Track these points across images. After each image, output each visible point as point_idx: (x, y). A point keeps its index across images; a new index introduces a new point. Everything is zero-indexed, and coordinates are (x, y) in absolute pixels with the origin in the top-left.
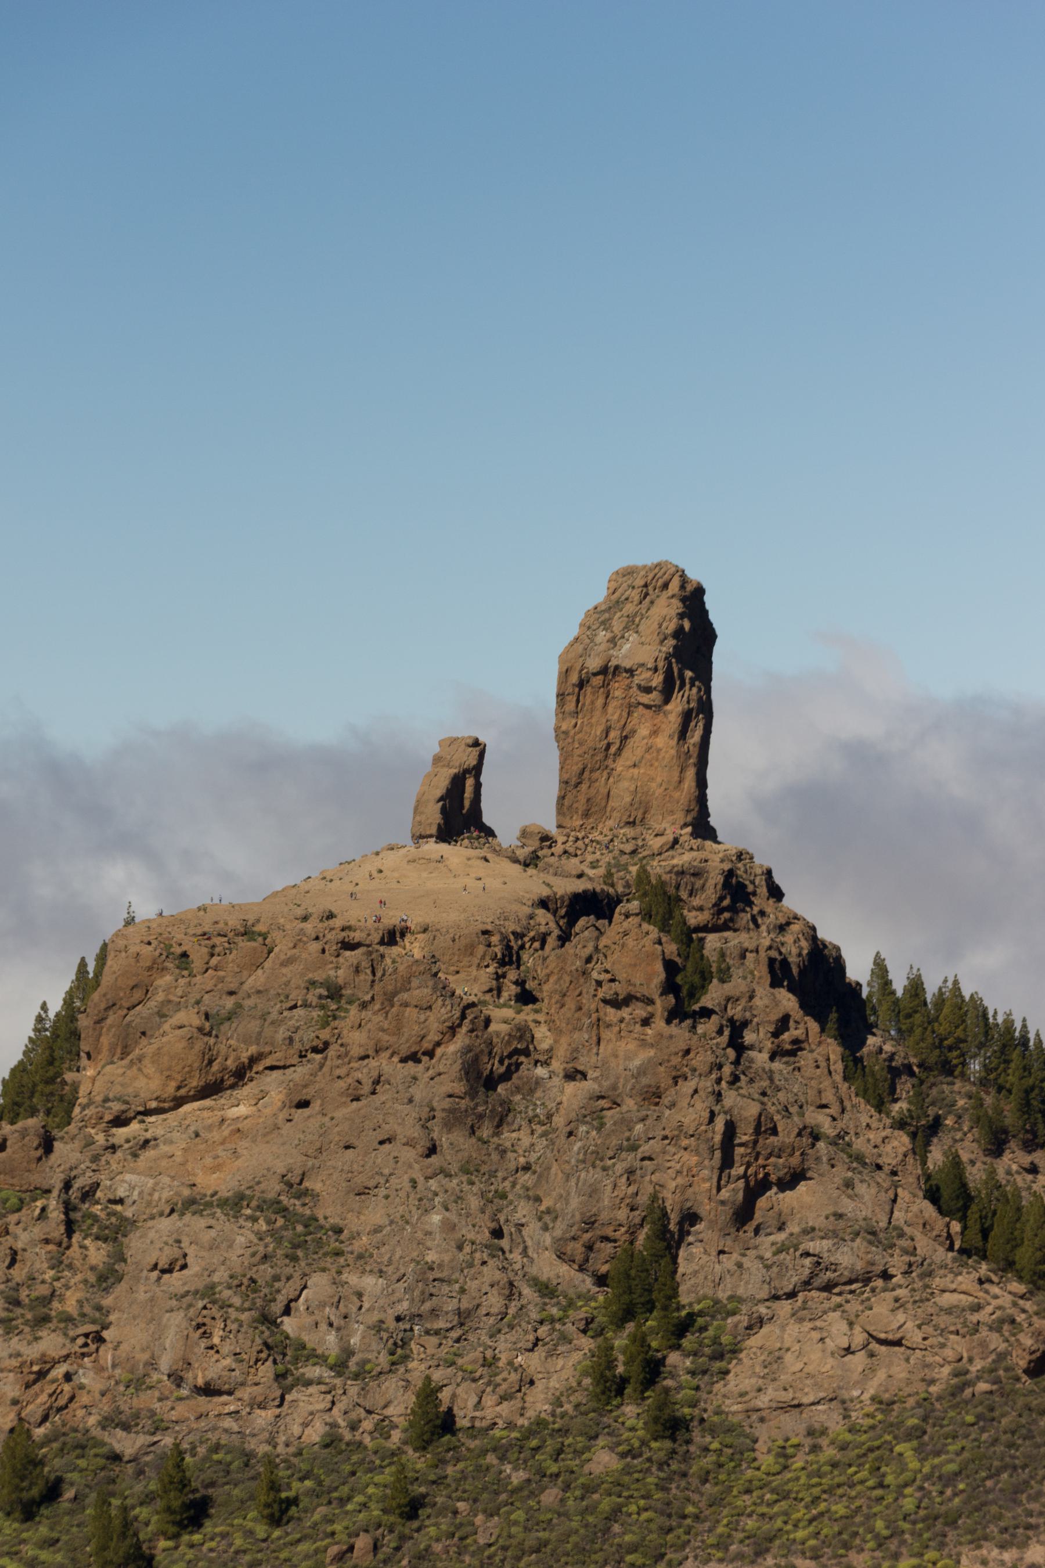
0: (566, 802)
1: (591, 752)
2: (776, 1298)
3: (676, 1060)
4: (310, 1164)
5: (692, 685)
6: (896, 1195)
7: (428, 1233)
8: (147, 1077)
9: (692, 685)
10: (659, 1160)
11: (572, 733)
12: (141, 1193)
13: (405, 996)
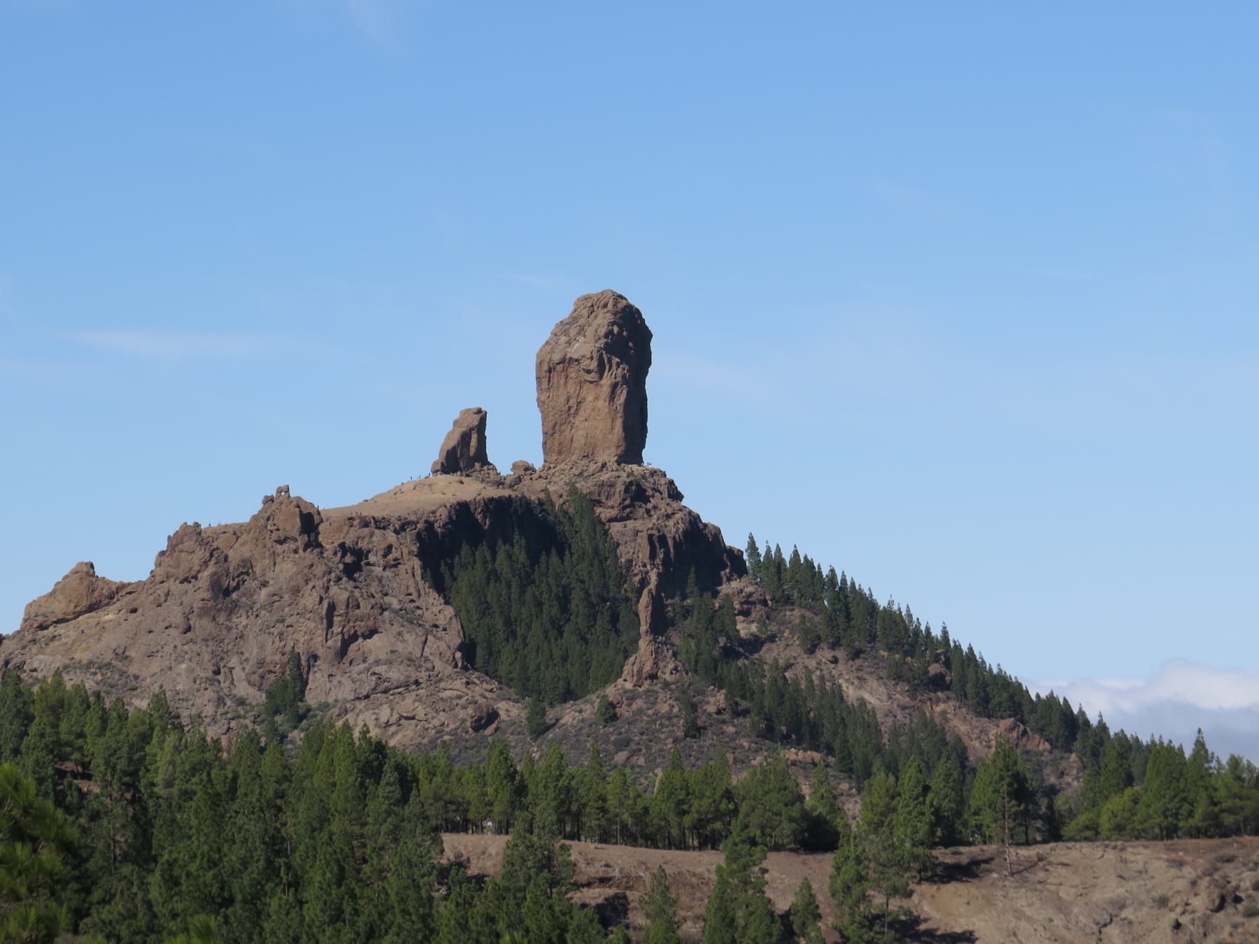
2: (359, 699)
3: (306, 571)
4: (129, 642)
5: (618, 366)
6: (426, 639)
7: (179, 674)
8: (59, 602)
9: (618, 366)
10: (295, 627)
11: (547, 402)
12: (45, 664)
13: (181, 546)
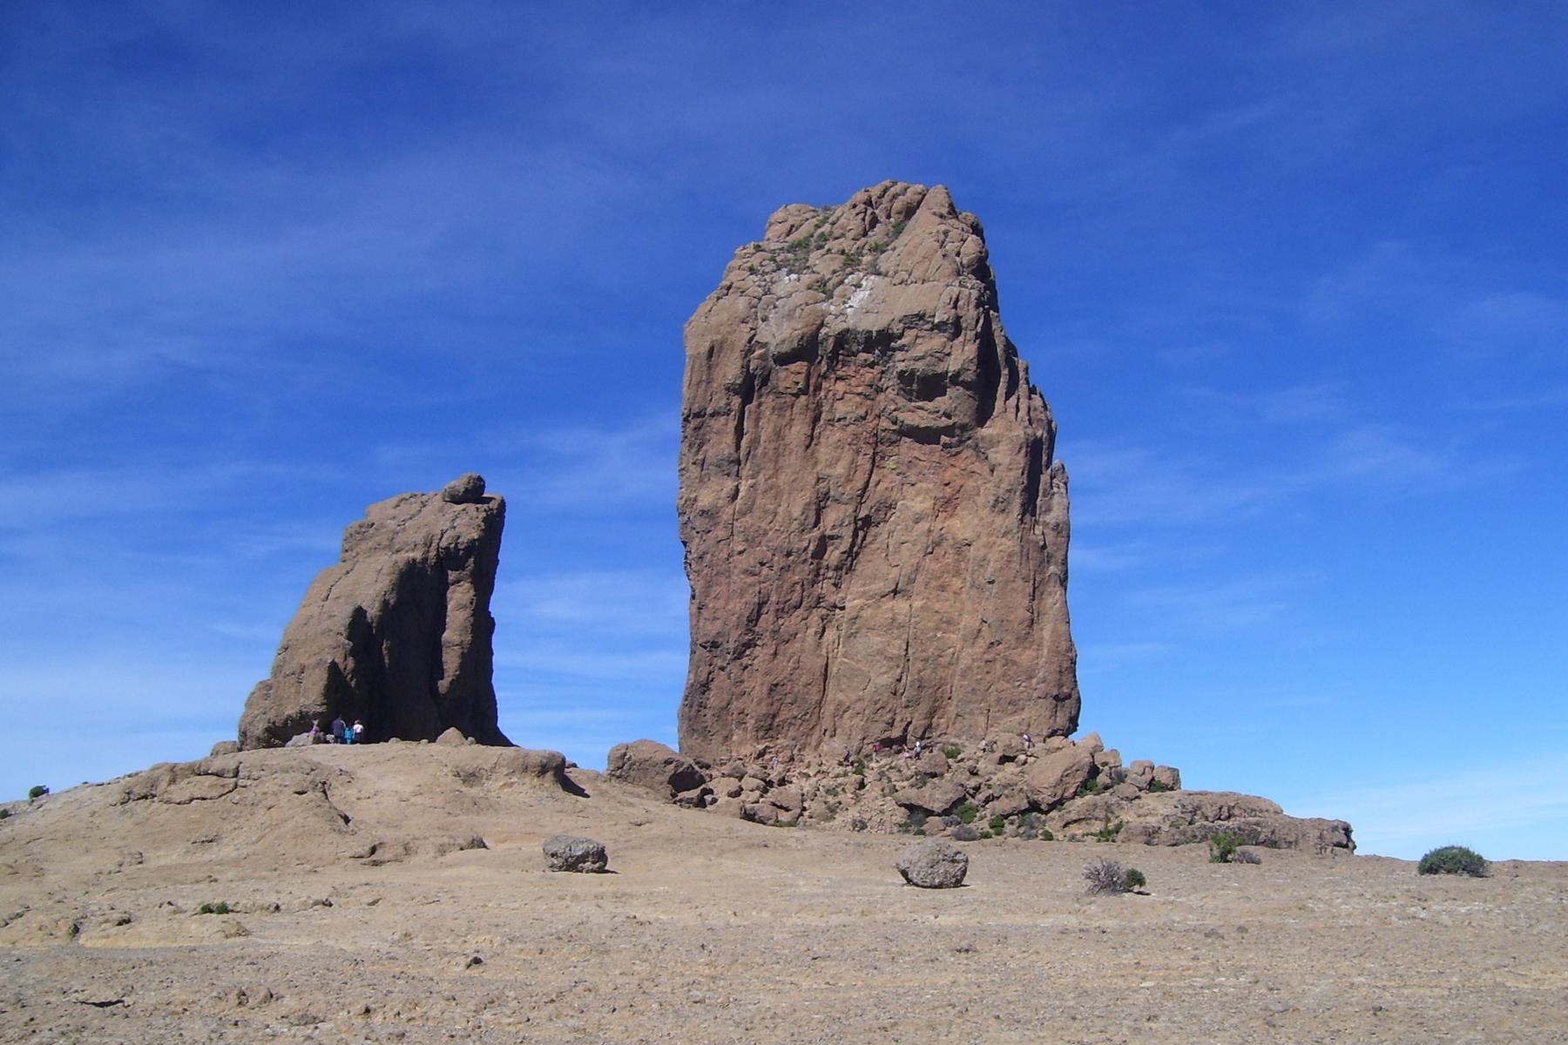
0: (714, 699)
1: (778, 561)
11: (726, 516)
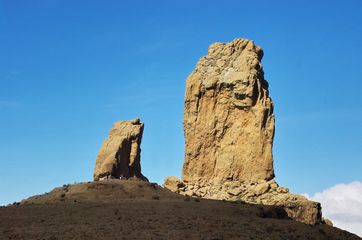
0: (190, 167)
1: (206, 136)
11: (194, 125)
